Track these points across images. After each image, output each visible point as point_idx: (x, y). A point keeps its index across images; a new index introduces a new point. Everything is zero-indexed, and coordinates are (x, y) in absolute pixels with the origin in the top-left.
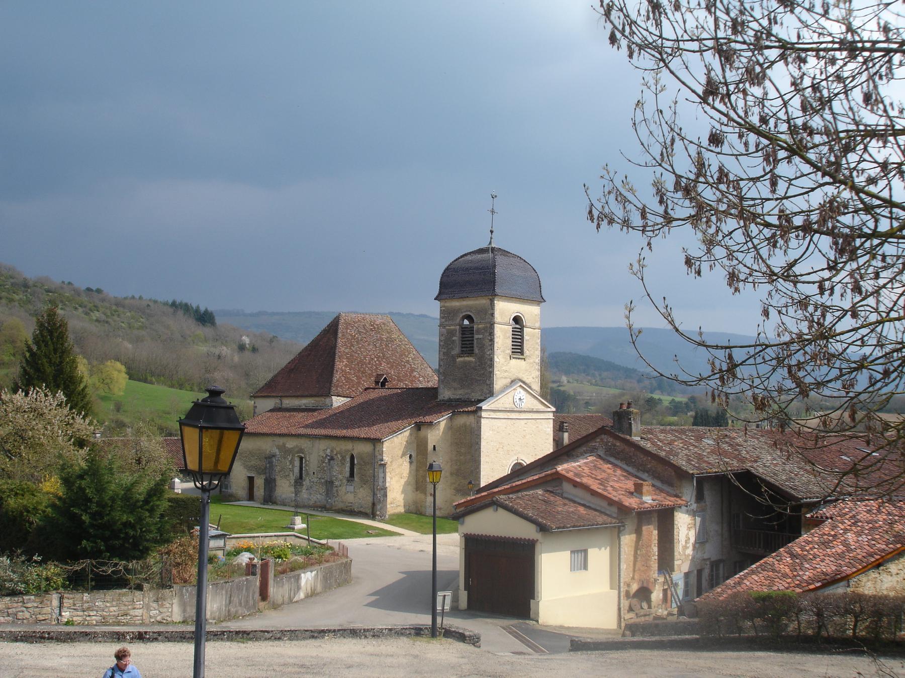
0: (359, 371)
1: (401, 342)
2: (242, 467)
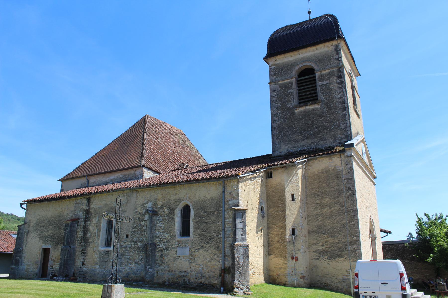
0: (164, 157)
1: (193, 149)
2: (38, 239)
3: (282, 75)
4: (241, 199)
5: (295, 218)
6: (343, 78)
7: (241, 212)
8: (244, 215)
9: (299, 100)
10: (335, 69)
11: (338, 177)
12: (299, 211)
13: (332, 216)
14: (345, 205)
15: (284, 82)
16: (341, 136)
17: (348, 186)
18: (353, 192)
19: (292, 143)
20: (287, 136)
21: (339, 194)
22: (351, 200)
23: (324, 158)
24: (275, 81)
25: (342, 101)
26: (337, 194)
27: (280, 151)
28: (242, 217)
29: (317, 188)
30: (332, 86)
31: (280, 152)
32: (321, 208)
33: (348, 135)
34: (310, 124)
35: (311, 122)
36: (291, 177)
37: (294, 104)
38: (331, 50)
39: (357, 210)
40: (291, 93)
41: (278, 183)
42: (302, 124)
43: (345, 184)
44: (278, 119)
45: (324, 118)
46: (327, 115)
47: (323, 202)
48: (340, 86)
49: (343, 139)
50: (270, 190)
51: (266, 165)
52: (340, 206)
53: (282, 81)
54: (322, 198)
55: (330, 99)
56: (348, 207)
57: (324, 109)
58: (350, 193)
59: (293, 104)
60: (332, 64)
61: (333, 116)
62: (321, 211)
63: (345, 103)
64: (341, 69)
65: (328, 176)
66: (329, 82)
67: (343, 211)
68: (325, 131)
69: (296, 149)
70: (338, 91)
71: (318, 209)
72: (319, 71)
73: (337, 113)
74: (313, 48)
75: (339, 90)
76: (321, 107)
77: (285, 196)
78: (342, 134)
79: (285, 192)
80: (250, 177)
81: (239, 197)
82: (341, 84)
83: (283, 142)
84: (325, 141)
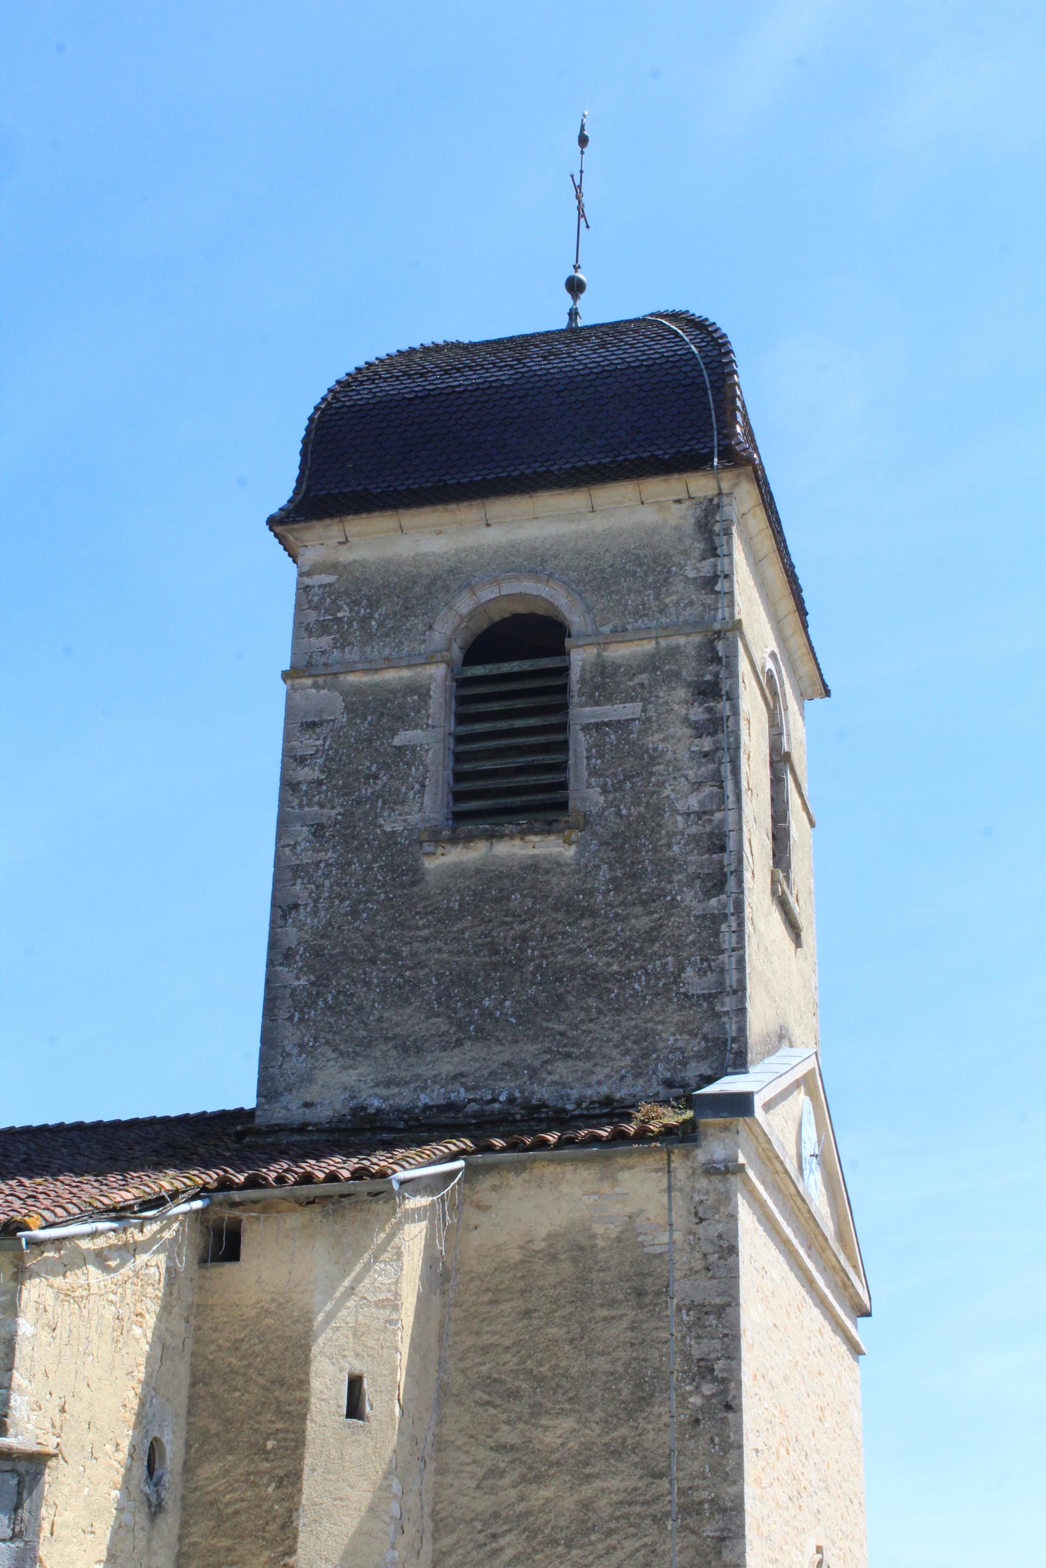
3: (369, 637)
4: (25, 1383)
5: (359, 1532)
6: (728, 699)
7: (13, 1471)
8: (30, 1493)
9: (458, 797)
10: (688, 642)
11: (640, 1294)
12: (384, 1488)
13: (584, 1535)
14: (669, 1467)
15: (377, 678)
16: (680, 1044)
17: (696, 1353)
18: (725, 1392)
19: (384, 1055)
20: (360, 1009)
21: (642, 1401)
22: (712, 1440)
23: (569, 1168)
24: (326, 665)
25: (711, 835)
26: (625, 1394)
27: (308, 1098)
28: (18, 1506)
29: (507, 1349)
30: (657, 737)
31: (307, 1105)
32: (523, 1479)
33: (725, 1043)
34: (507, 951)
35: (514, 940)
36: (358, 1268)
37: (423, 820)
38: (677, 528)
39: (737, 1508)
40: (413, 749)
41: (268, 1297)
42: (455, 946)
43: (684, 1337)
44: (316, 901)
45: (594, 926)
46: (609, 905)
47: (541, 1442)
48: (707, 744)
49: (693, 1064)
50: (214, 1336)
51: (211, 1177)
52: (639, 1472)
53: (366, 671)
54: (532, 1415)
55: (641, 818)
56: (685, 1484)
57: (598, 867)
58: (703, 1396)
59: (414, 818)
60: (672, 610)
61: (646, 919)
62: (522, 1498)
63: (723, 849)
64: (720, 646)
65: (583, 1280)
66: (644, 710)
67: (655, 1509)
68: (592, 1002)
69: (404, 1097)
70: (691, 774)
71: (506, 1481)
72: (589, 640)
73: (674, 904)
74: (574, 500)
75: (700, 765)
76: (580, 854)
77: (304, 1383)
78: (690, 1033)
79: (307, 1361)
80: (101, 1242)
81: (10, 1369)
82: (713, 734)
83: (328, 1043)
84: (582, 1065)
